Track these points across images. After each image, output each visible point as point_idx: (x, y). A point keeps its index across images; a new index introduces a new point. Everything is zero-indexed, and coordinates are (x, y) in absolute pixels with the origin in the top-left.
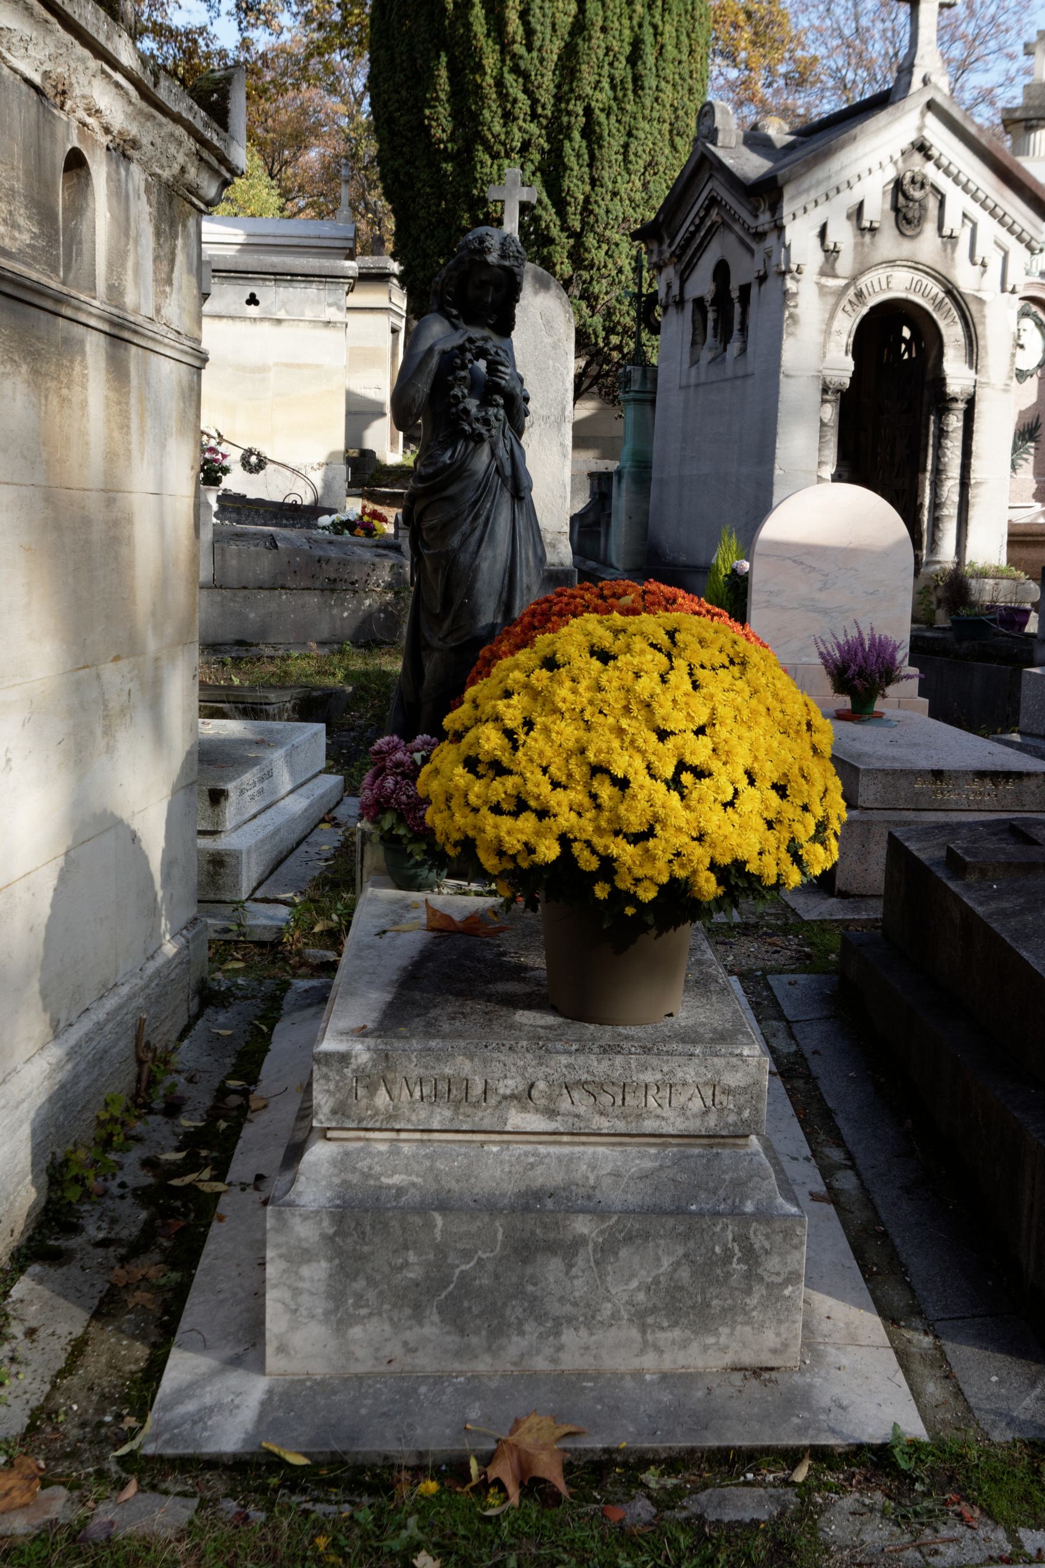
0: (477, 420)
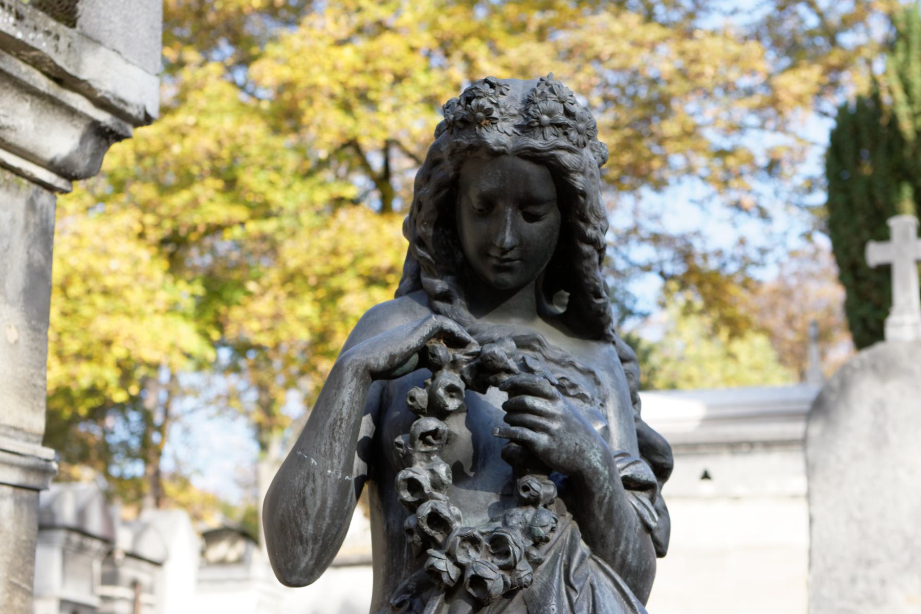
0: (473, 541)
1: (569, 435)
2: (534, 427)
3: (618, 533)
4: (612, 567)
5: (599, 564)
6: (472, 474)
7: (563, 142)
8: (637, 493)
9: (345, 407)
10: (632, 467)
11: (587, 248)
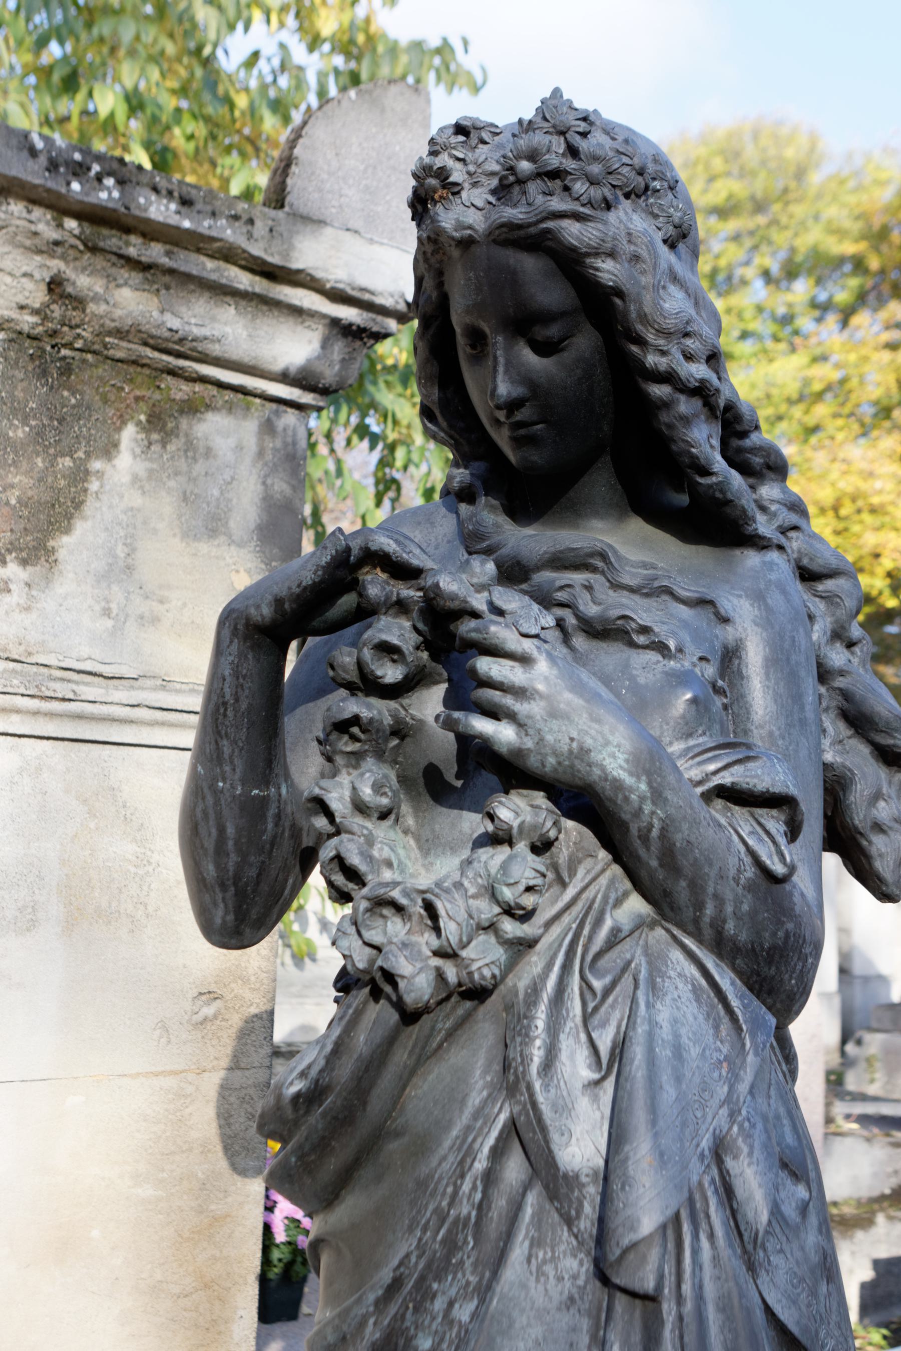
1: (555, 724)
2: (493, 713)
3: (696, 888)
4: (700, 941)
5: (674, 937)
6: (459, 784)
7: (557, 204)
8: (759, 811)
9: (227, 685)
10: (736, 769)
11: (659, 391)
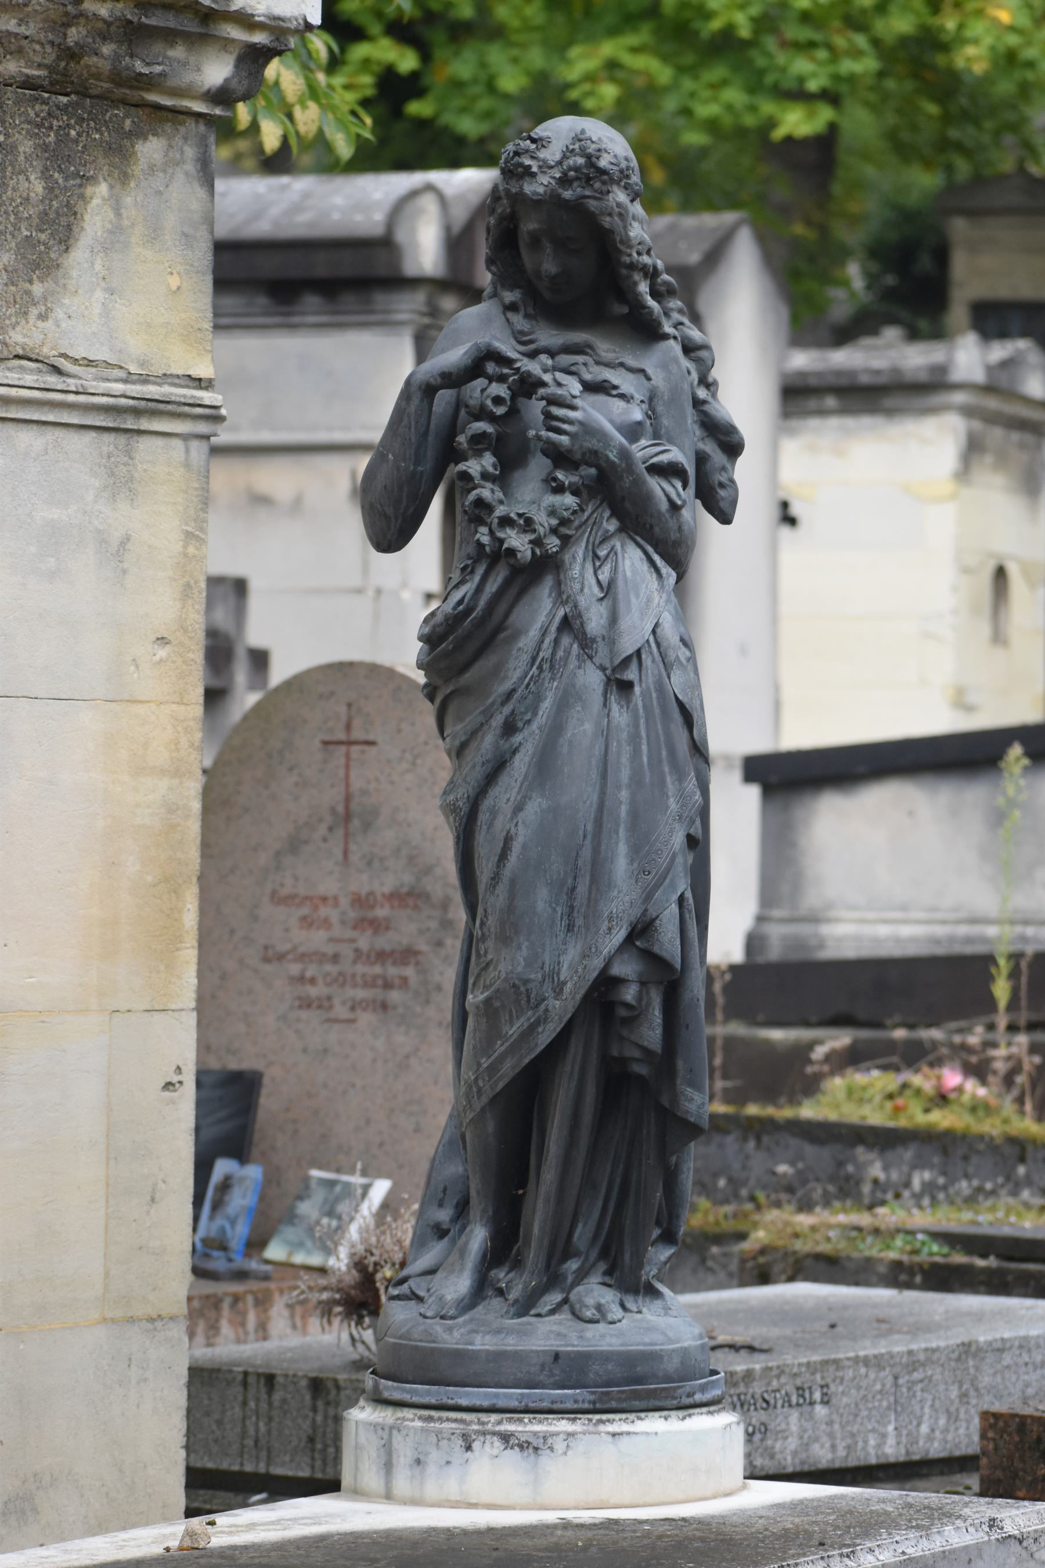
2: (559, 431)
7: (587, 193)
